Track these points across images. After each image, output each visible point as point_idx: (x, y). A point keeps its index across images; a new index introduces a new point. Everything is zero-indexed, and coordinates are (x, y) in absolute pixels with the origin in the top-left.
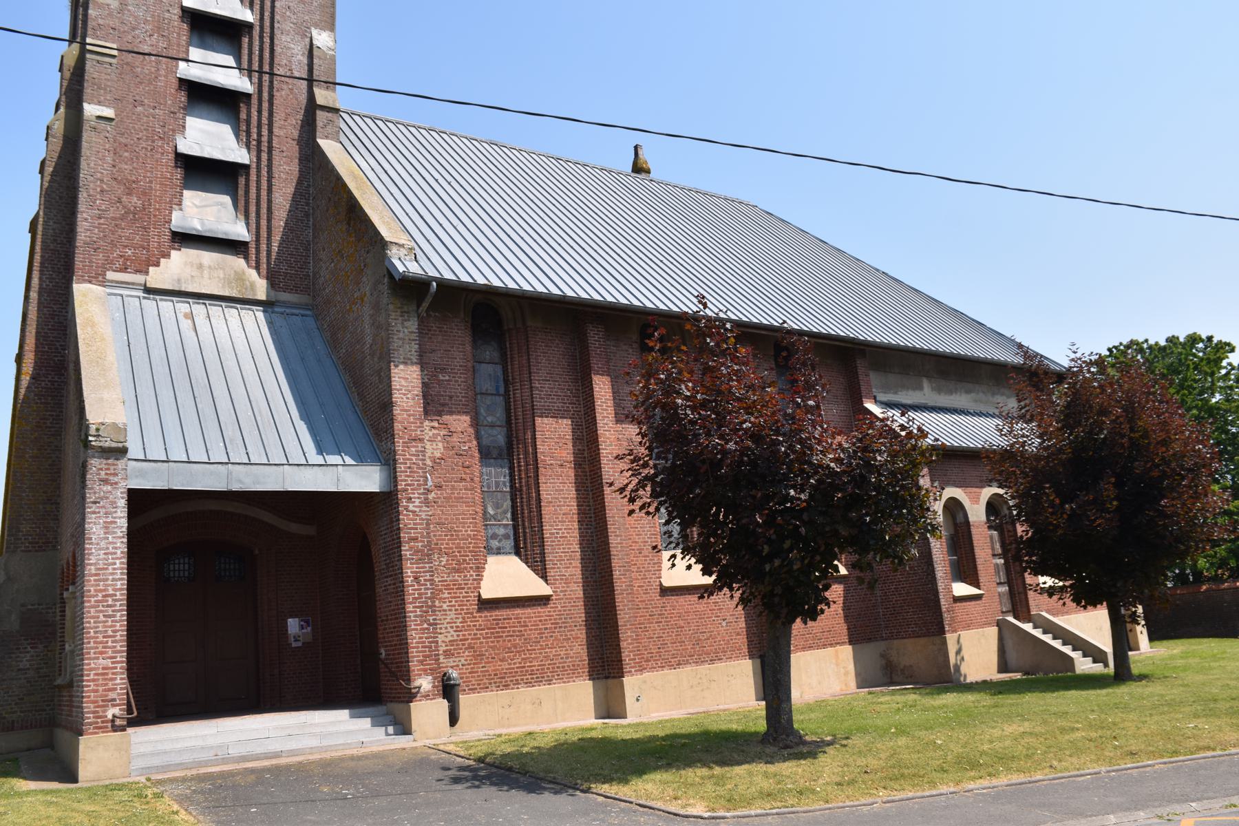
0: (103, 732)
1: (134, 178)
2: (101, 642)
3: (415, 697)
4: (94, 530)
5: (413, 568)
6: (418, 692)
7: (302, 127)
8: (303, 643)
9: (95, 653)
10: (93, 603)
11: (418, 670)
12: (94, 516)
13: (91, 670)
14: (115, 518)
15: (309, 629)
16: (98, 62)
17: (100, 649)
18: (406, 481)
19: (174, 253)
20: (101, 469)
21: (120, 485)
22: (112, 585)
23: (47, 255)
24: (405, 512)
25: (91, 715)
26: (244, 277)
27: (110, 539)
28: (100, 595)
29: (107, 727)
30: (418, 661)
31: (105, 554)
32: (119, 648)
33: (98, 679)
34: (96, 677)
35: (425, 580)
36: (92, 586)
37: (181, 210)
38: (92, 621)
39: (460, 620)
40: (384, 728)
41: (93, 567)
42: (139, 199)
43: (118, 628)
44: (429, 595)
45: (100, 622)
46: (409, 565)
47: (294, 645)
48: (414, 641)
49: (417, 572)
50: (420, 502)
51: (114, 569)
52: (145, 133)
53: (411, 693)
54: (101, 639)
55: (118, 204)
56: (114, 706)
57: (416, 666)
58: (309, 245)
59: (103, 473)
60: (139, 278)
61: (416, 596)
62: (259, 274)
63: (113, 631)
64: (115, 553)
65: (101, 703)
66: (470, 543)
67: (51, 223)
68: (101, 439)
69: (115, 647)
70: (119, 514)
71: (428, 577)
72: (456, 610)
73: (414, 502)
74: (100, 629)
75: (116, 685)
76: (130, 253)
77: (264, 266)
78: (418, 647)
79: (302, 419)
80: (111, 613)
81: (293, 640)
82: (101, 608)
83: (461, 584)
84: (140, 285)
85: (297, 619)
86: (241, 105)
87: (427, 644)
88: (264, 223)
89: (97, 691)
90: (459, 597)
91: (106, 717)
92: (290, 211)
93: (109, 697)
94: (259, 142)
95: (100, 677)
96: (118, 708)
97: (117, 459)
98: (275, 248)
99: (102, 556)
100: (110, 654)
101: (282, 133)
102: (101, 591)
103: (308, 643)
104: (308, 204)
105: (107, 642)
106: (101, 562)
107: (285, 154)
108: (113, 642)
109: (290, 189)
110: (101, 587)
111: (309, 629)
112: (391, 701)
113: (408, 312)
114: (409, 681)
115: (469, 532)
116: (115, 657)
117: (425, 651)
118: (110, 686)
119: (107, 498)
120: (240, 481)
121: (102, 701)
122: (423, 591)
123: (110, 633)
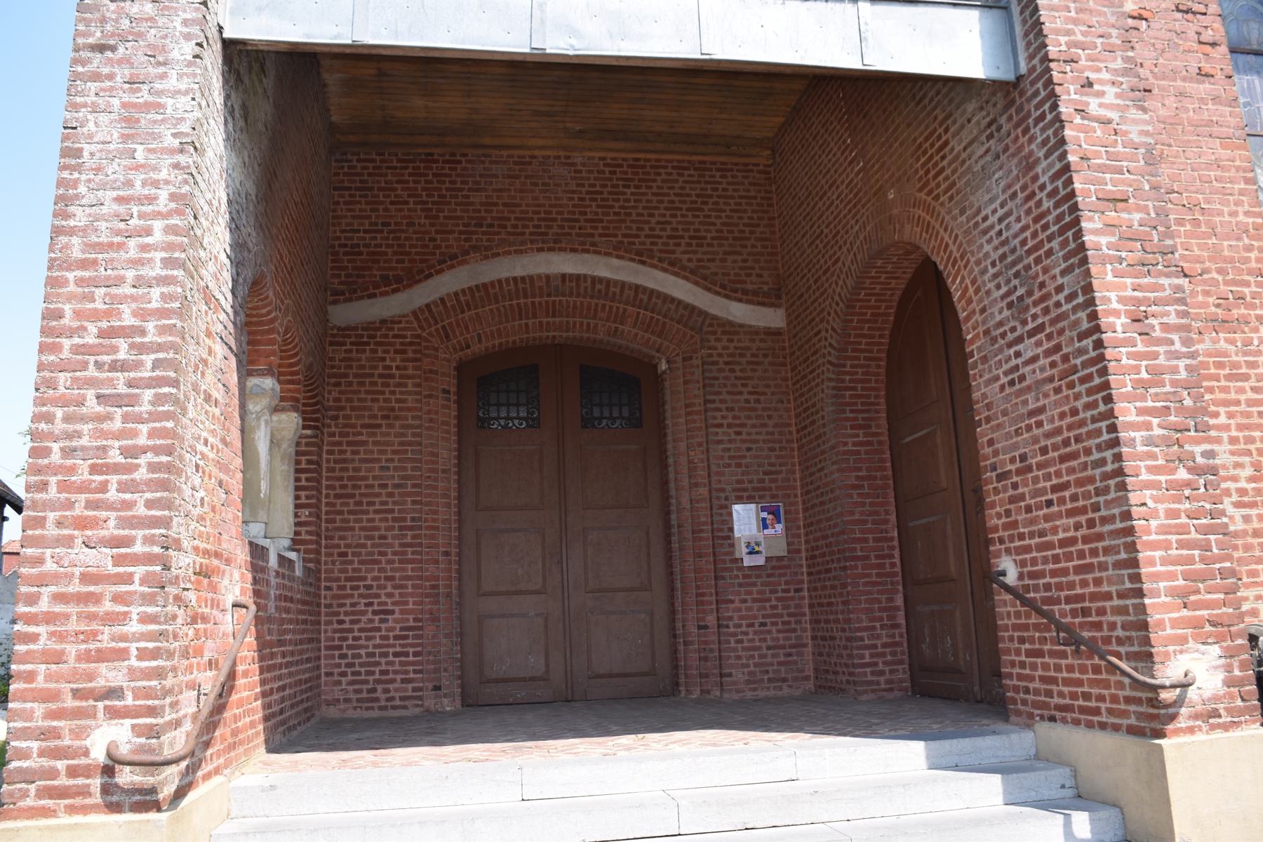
0: (71, 810)
2: (83, 488)
3: (1173, 717)
4: (91, 125)
5: (1124, 287)
6: (1179, 702)
8: (768, 559)
9: (59, 524)
10: (65, 354)
11: (1175, 623)
12: (93, 86)
13: (42, 581)
14: (160, 93)
15: (779, 527)
17: (78, 510)
18: (1068, 33)
22: (134, 298)
24: (1078, 120)
25: (35, 745)
27: (140, 155)
28: (92, 329)
29: (84, 792)
30: (1172, 592)
31: (119, 200)
32: (141, 510)
33: (67, 617)
34: (58, 608)
35: (1166, 327)
36: (70, 298)
38: (59, 413)
39: (1249, 471)
40: (1059, 819)
41: (75, 240)
43: (142, 441)
44: (1183, 375)
45: (83, 419)
46: (1110, 277)
47: (748, 561)
48: (1154, 523)
49: (1138, 302)
50: (1118, 96)
51: (144, 248)
53: (1154, 702)
54: (83, 475)
56: (114, 714)
57: (1166, 608)
61: (1144, 375)
63: (125, 451)
64: (151, 200)
65: (70, 703)
66: (1249, 249)
69: (128, 505)
70: (172, 82)
71: (1173, 319)
72: (1233, 440)
73: (1101, 94)
74: (85, 441)
75: (124, 638)
78: (1166, 546)
80: (122, 389)
81: (745, 550)
82: (92, 372)
83: (1235, 365)
85: (753, 506)
87: (1194, 535)
89: (56, 658)
90: (1238, 403)
91: (86, 753)
93: (100, 683)
95: (72, 609)
96: (128, 722)
99: (110, 208)
100: (112, 528)
102: (95, 316)
103: (780, 559)
105: (103, 488)
106: (103, 225)
108: (123, 488)
110: (99, 305)
111: (779, 527)
112: (1052, 719)
114: (1146, 657)
115: (1241, 218)
116: (127, 542)
117: (1190, 560)
118: (105, 640)
119: (140, 35)
121: (76, 694)
122: (1162, 360)
123: (115, 457)
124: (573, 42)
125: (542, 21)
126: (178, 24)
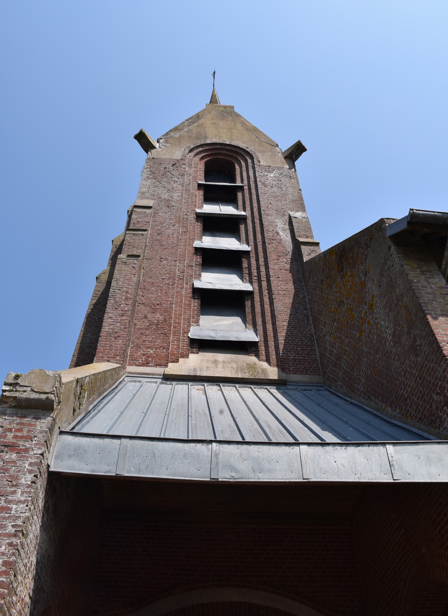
1: (158, 302)
7: (292, 262)
14: (10, 502)
16: (134, 234)
19: (191, 356)
20: (10, 430)
21: (31, 453)
23: (82, 357)
26: (255, 366)
37: (198, 325)
42: (162, 315)
52: (168, 275)
55: (144, 319)
58: (313, 337)
59: (10, 435)
60: (160, 370)
62: (269, 363)
67: (89, 335)
68: (18, 388)
70: (18, 496)
76: (152, 352)
77: (273, 357)
79: (323, 429)
84: (160, 375)
86: (243, 259)
88: (269, 327)
92: (291, 315)
94: (259, 276)
97: (37, 418)
98: (281, 340)
101: (276, 267)
104: (306, 309)
107: (280, 279)
109: (289, 300)
113: (429, 272)
120: (233, 469)
124: (233, 474)
125: (217, 464)
126: (26, 465)
